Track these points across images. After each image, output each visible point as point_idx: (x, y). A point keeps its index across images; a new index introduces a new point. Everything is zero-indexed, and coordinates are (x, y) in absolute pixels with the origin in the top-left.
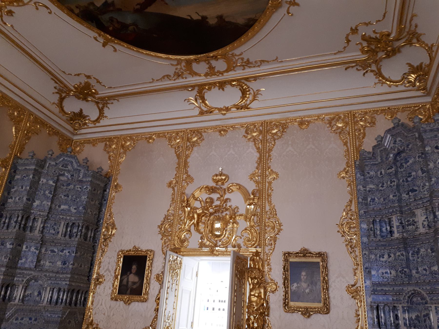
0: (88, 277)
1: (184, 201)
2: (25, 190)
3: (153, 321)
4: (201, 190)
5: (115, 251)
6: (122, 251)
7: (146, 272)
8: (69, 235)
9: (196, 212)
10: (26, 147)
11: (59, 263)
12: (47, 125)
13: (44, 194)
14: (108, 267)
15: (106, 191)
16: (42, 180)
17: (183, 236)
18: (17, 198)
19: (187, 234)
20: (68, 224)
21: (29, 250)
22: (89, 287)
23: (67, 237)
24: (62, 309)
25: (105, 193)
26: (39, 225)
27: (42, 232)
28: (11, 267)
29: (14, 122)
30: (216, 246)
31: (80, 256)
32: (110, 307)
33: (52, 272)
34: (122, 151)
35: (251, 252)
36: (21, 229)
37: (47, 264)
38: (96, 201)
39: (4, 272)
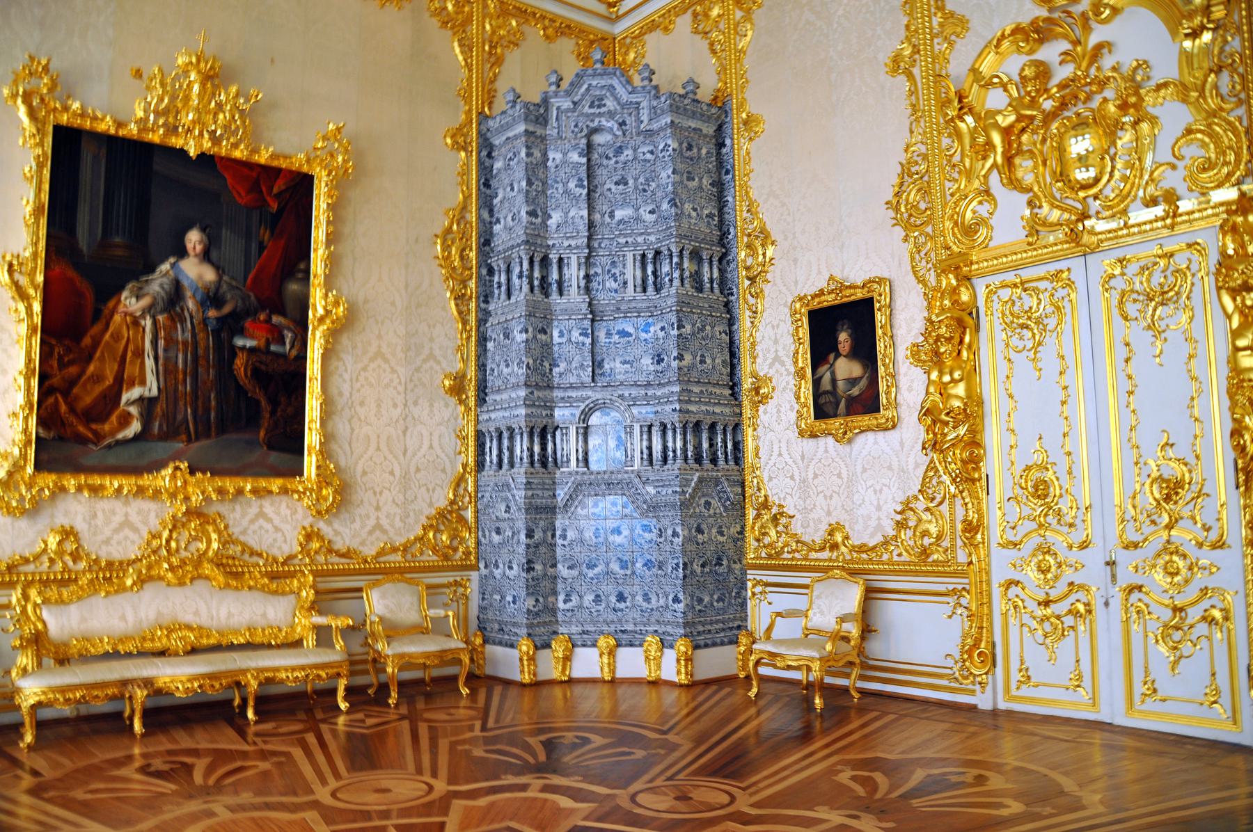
0: (732, 388)
1: (947, 103)
2: (519, 191)
3: (924, 479)
4: (997, 47)
5: (785, 305)
6: (801, 299)
7: (880, 346)
8: (655, 283)
9: (996, 125)
10: (498, 84)
11: (647, 361)
12: (534, 14)
13: (567, 192)
14: (776, 351)
15: (723, 145)
16: (551, 155)
17: (969, 215)
18: (509, 218)
19: (980, 203)
20: (644, 256)
21: (570, 340)
22: (741, 414)
23: (650, 289)
24: (677, 472)
25: (724, 151)
26: (574, 273)
27: (588, 290)
28: (537, 386)
29: (452, 28)
30: (1084, 216)
31: (693, 334)
32: (803, 457)
33: (636, 385)
34: (739, 14)
35: (1222, 204)
36: (537, 290)
37: (618, 366)
38: (701, 179)
39: (525, 399)
